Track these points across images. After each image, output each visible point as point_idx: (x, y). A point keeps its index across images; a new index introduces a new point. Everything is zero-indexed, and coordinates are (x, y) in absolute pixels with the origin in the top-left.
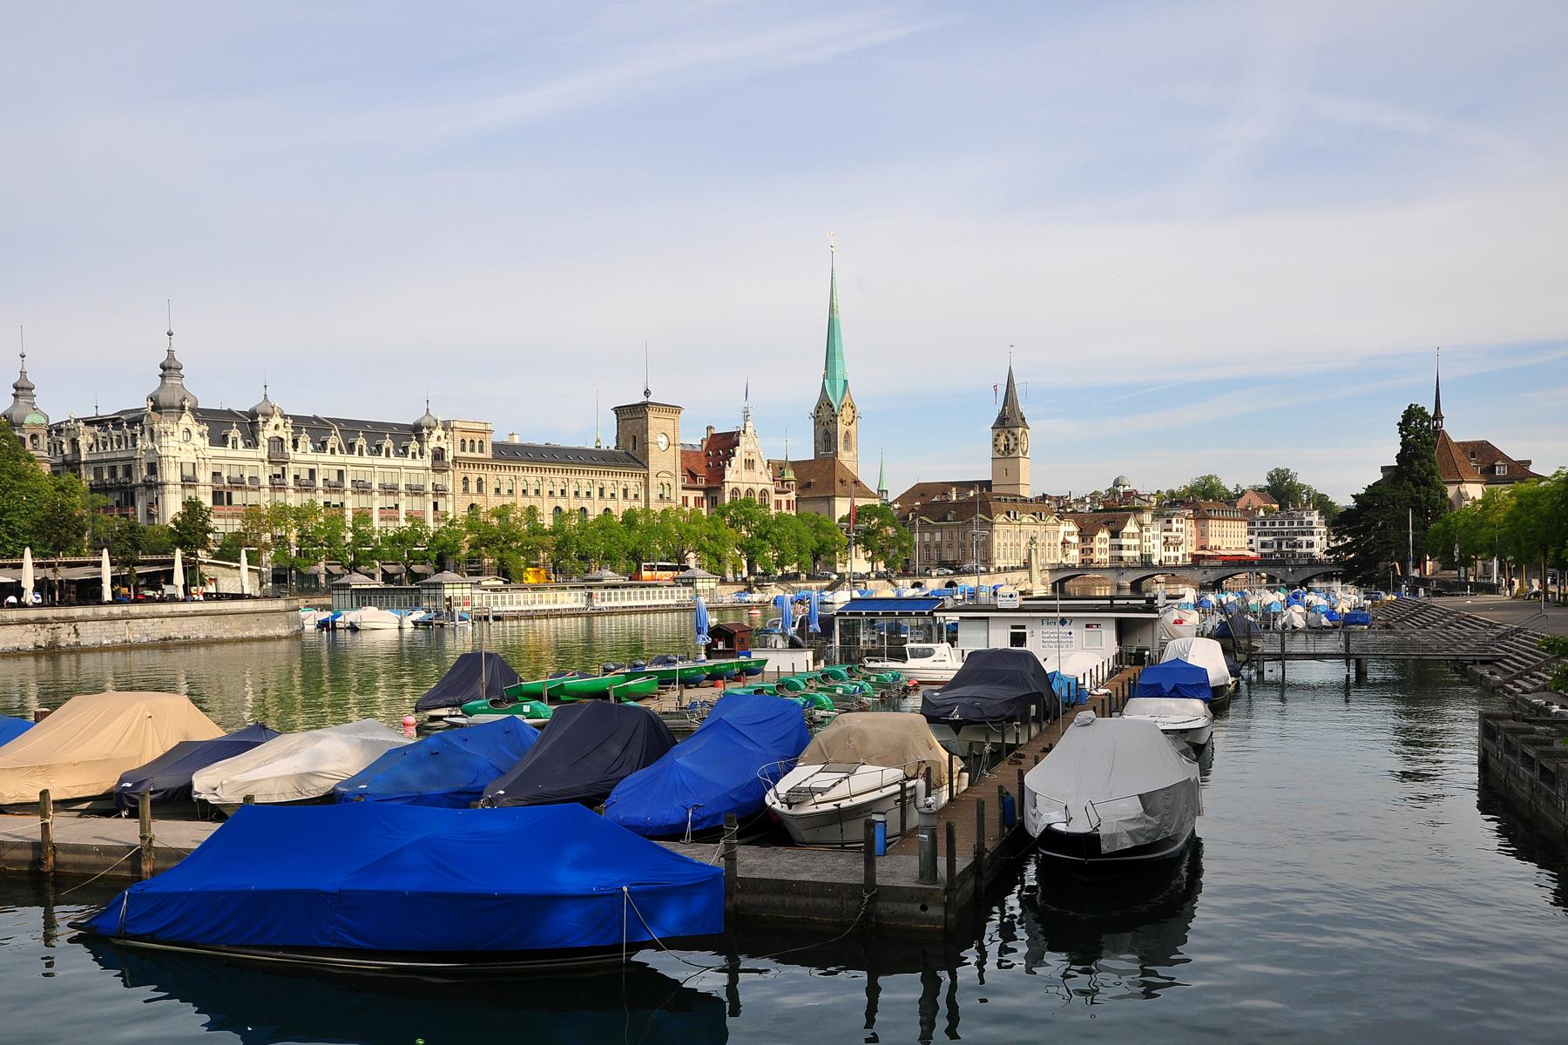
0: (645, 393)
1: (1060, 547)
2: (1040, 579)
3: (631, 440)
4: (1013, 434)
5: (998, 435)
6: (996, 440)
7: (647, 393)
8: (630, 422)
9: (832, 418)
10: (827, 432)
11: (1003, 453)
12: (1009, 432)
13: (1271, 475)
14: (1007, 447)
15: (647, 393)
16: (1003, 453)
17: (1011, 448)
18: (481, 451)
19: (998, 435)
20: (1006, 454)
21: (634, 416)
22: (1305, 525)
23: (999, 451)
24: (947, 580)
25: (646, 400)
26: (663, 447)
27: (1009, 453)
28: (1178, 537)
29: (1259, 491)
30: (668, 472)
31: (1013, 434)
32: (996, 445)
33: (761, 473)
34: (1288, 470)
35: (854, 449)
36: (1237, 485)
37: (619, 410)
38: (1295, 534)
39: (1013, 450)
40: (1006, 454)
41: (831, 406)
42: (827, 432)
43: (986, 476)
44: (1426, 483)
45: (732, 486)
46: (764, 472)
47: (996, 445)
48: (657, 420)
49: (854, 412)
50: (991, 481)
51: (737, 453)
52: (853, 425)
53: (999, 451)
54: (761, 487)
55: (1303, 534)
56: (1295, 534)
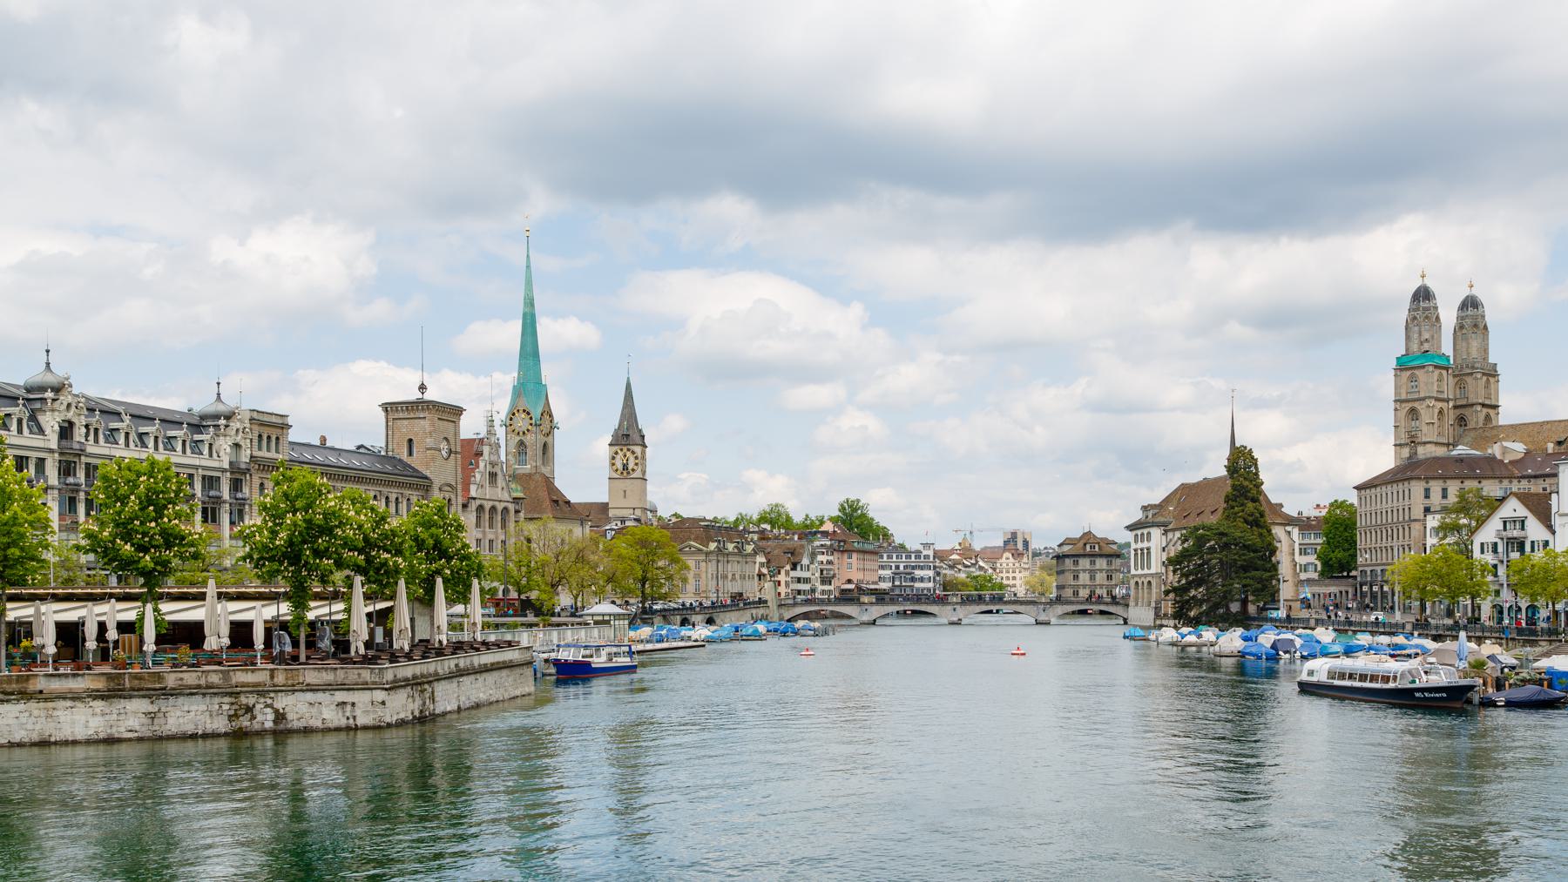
0: (420, 388)
1: (756, 578)
2: (778, 615)
3: (406, 444)
4: (633, 453)
5: (616, 453)
6: (613, 458)
7: (422, 388)
8: (406, 422)
9: (530, 427)
10: (521, 443)
11: (622, 473)
12: (628, 450)
13: (842, 505)
14: (625, 467)
15: (422, 388)
16: (622, 473)
17: (630, 467)
18: (277, 451)
19: (616, 453)
20: (625, 474)
21: (412, 415)
22: (922, 559)
23: (617, 470)
24: (708, 616)
25: (421, 396)
26: (445, 455)
27: (628, 473)
28: (830, 570)
29: (834, 520)
30: (450, 485)
31: (633, 453)
32: (613, 464)
33: (503, 488)
34: (858, 501)
35: (551, 464)
36: (807, 516)
37: (388, 408)
38: (913, 568)
39: (633, 470)
40: (625, 474)
41: (528, 413)
42: (521, 443)
43: (605, 499)
44: (1258, 525)
45: (478, 502)
46: (505, 487)
47: (613, 464)
48: (441, 422)
49: (551, 421)
50: (607, 504)
51: (482, 464)
52: (550, 436)
53: (617, 470)
54: (503, 505)
55: (922, 568)
56: (913, 568)
